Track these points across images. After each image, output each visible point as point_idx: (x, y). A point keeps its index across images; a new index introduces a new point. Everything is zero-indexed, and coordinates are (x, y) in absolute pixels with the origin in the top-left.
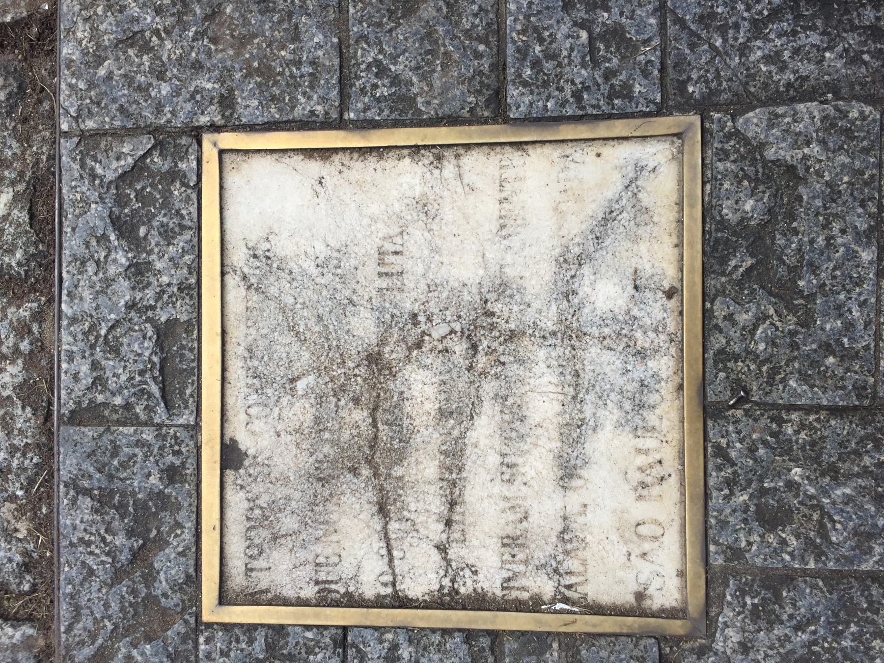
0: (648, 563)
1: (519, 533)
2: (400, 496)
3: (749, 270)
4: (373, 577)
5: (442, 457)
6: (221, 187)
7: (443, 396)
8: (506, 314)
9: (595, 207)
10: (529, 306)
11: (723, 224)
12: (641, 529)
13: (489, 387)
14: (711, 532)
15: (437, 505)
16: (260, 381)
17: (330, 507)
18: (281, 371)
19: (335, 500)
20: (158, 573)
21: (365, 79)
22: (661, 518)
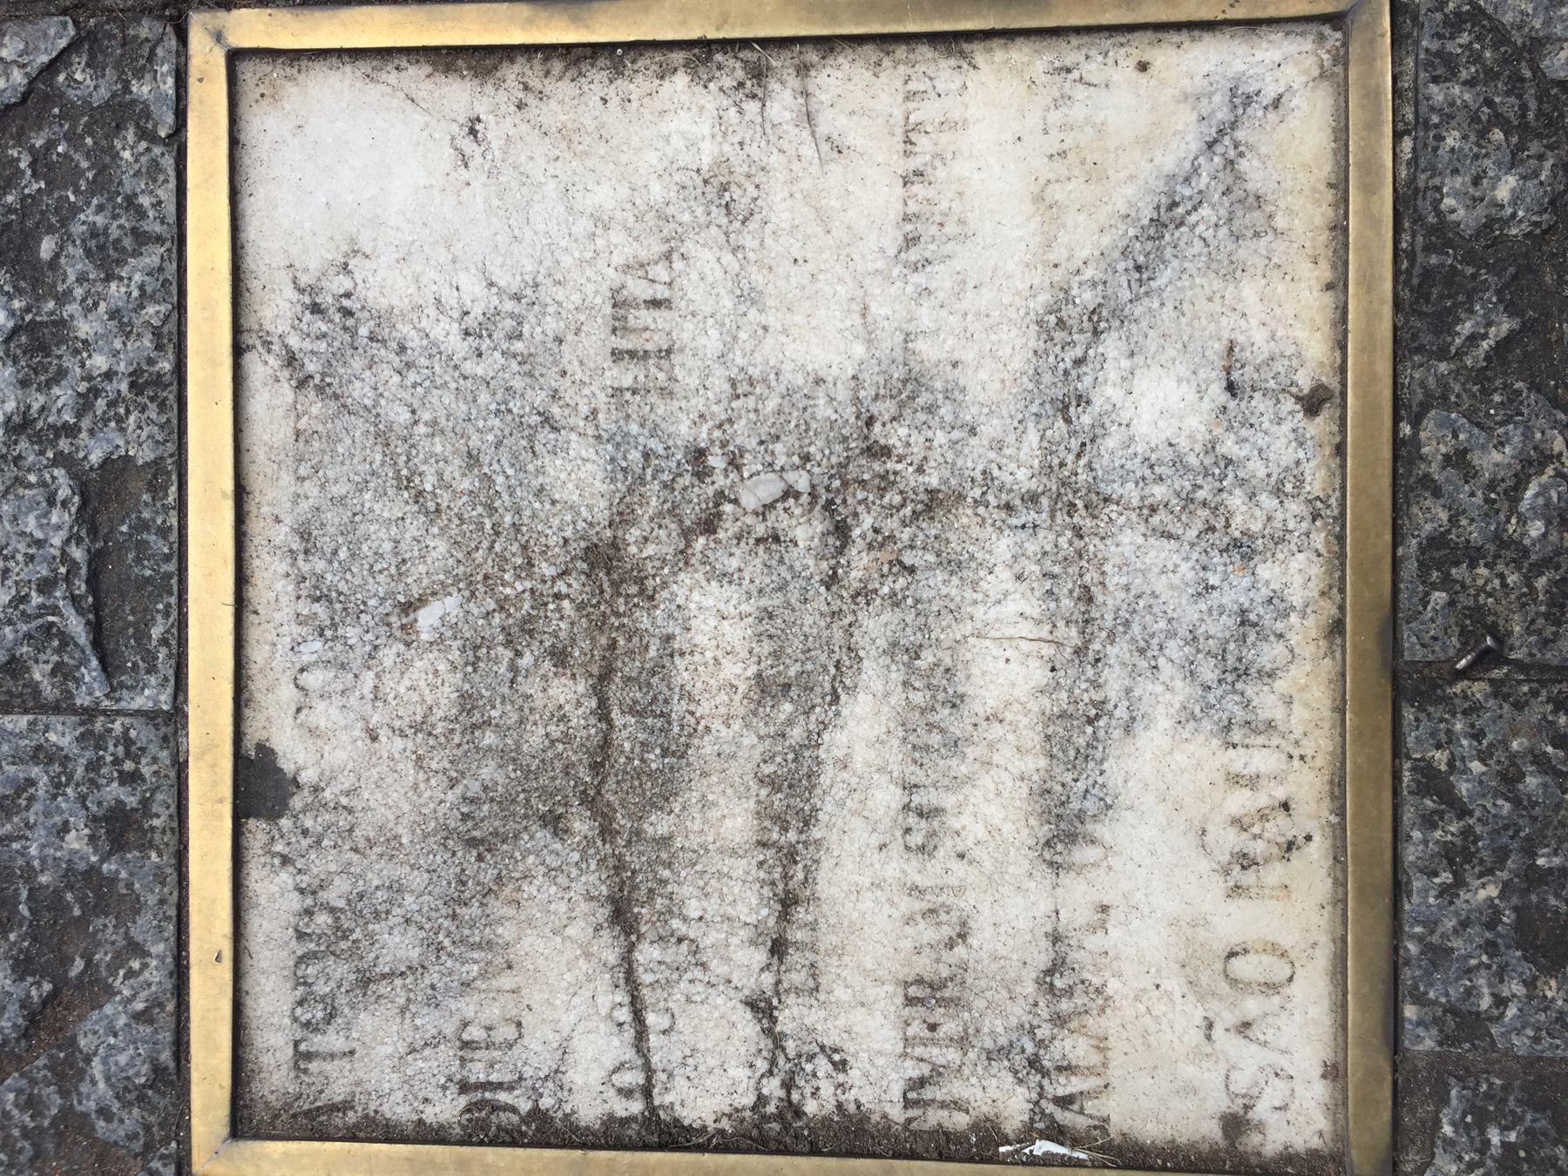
0: (1254, 1047)
1: (945, 973)
2: (663, 882)
3: (1504, 346)
4: (597, 1075)
5: (764, 792)
6: (234, 142)
7: (767, 647)
8: (918, 451)
9: (1131, 192)
10: (973, 432)
11: (1442, 234)
12: (1239, 966)
13: (876, 625)
14: (1407, 974)
16: (330, 608)
17: (497, 907)
18: (381, 585)
19: (508, 890)
20: (88, 1060)
22: (1286, 941)
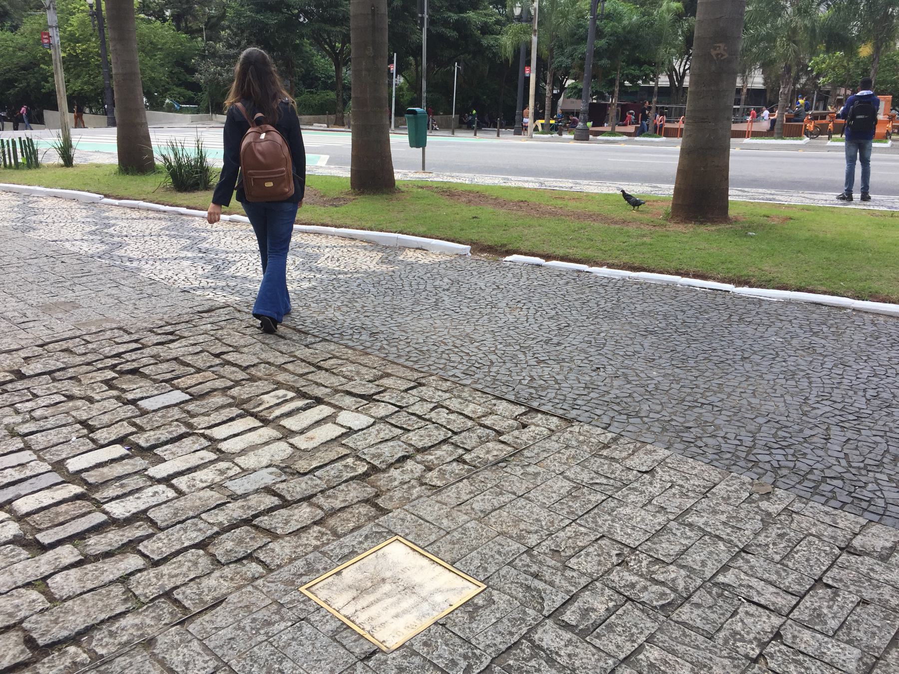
9: (453, 587)
13: (399, 596)
21: (435, 546)
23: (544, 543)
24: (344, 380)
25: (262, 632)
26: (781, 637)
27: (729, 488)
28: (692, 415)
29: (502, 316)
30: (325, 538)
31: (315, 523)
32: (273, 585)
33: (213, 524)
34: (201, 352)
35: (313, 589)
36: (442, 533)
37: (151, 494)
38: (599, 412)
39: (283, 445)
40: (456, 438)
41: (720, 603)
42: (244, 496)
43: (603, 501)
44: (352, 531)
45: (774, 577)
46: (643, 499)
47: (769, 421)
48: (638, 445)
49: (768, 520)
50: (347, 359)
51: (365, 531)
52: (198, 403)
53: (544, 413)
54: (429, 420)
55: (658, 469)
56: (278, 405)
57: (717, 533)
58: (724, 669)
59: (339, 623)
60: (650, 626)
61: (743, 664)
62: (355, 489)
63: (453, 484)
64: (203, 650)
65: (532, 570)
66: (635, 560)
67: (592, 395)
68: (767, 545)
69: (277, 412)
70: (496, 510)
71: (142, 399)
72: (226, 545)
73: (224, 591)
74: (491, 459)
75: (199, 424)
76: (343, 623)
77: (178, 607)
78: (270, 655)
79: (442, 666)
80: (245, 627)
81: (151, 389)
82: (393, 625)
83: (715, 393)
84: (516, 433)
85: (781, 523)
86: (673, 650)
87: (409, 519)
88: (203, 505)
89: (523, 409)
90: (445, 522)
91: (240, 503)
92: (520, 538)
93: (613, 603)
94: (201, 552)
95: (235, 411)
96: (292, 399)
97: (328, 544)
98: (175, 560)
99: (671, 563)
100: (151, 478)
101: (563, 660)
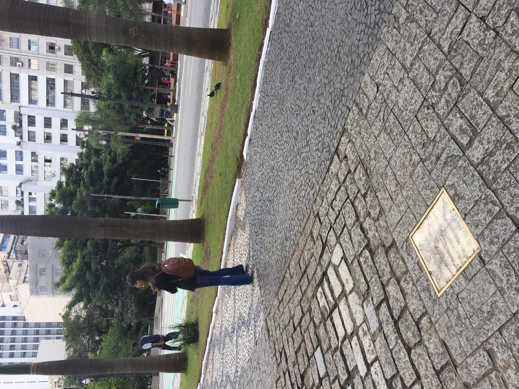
9: (442, 207)
13: (446, 239)
15: (450, 260)
21: (417, 216)
23: (418, 152)
24: (313, 259)
25: (464, 321)
26: (483, 17)
27: (390, 40)
28: (344, 58)
29: (279, 164)
30: (408, 279)
31: (399, 284)
32: (436, 312)
33: (396, 342)
34: (292, 338)
35: (439, 290)
36: (408, 210)
37: (376, 376)
38: (340, 113)
39: (350, 297)
40: (351, 197)
41: (460, 51)
42: (380, 323)
43: (394, 114)
44: (404, 262)
45: (446, 18)
46: (394, 91)
47: (350, 14)
48: (361, 91)
49: (411, 19)
50: (301, 255)
51: (405, 255)
52: (322, 343)
53: (338, 145)
54: (339, 211)
55: (376, 81)
56: (326, 298)
57: (417, 49)
58: (501, 52)
59: (461, 276)
60: (472, 94)
61: (499, 40)
62: (379, 259)
63: (379, 201)
64: (473, 356)
65: (435, 160)
66: (431, 99)
67: (329, 116)
68: (426, 21)
69: (330, 298)
70: (396, 178)
71: (319, 375)
72: (409, 336)
73: (437, 340)
74: (365, 178)
75: (336, 344)
76: (461, 273)
77: (445, 368)
78: (478, 317)
79: (491, 218)
80: (460, 331)
81: (313, 369)
82: (464, 244)
83: (331, 44)
84: (350, 162)
85: (414, 11)
86: (488, 81)
87: (399, 229)
88: (385, 347)
89: (336, 157)
90: (402, 208)
91: (384, 325)
92: (415, 165)
93: (457, 114)
94: (413, 351)
95: (329, 322)
96: (323, 289)
97: (412, 278)
98: (417, 367)
99: (435, 78)
100: (367, 375)
101: (491, 147)
